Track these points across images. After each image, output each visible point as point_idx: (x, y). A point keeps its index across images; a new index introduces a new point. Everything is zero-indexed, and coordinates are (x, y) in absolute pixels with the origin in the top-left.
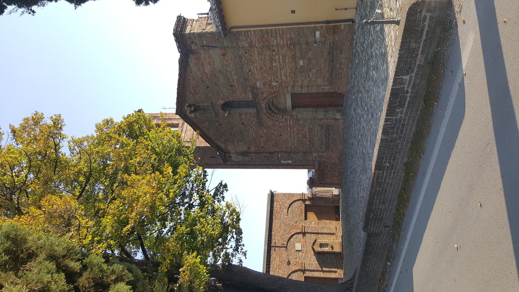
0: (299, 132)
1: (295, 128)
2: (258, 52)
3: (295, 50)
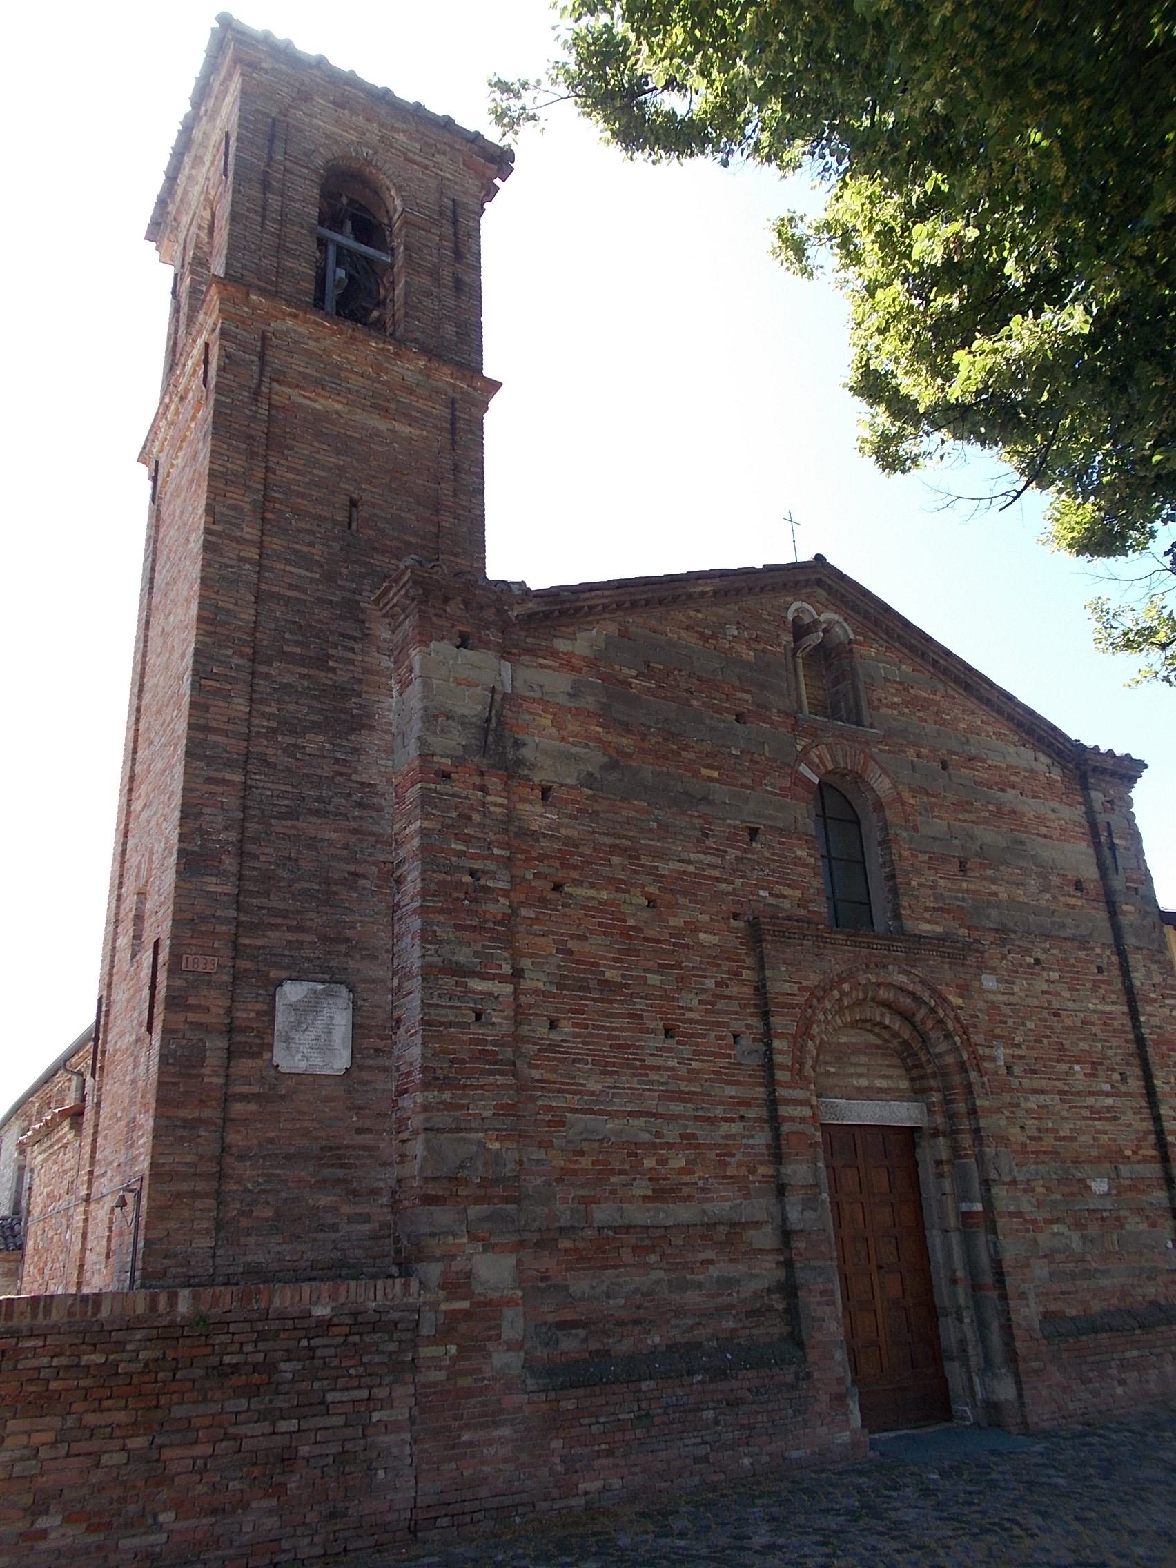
0: (711, 1155)
1: (735, 1128)
3: (1139, 1162)
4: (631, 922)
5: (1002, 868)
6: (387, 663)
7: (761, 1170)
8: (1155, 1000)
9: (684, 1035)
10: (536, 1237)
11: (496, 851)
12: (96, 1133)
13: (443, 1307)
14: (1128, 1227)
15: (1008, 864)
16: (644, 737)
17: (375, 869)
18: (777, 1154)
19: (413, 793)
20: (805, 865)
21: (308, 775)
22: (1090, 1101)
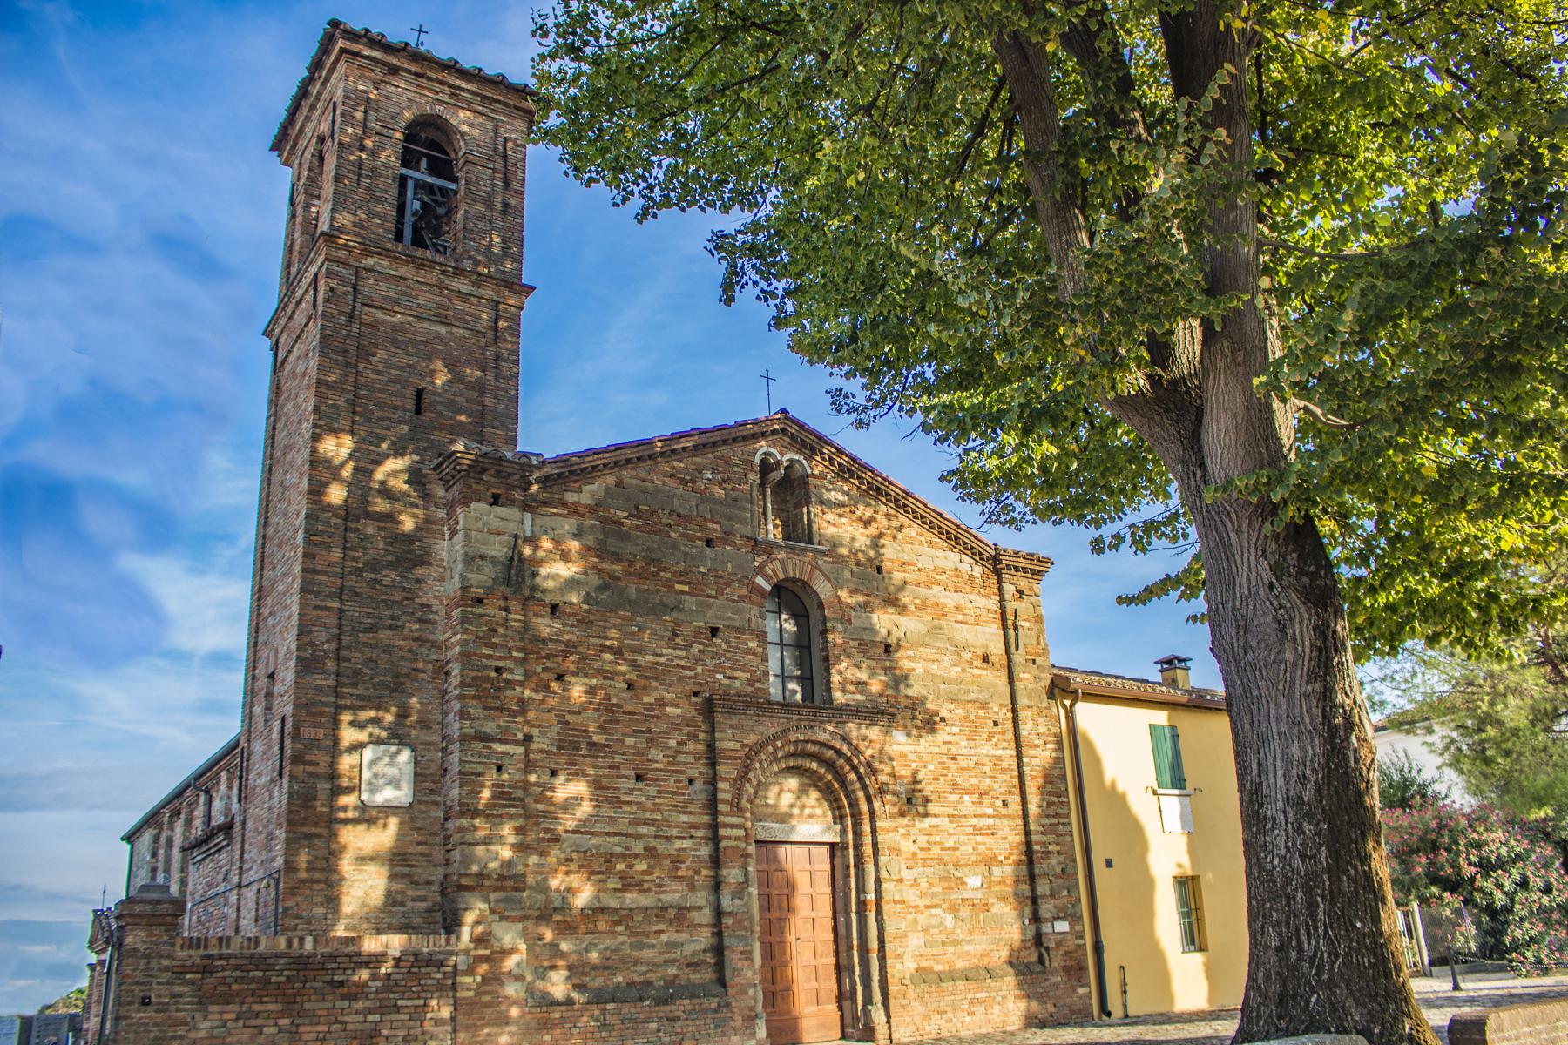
0: (667, 862)
1: (686, 844)
2: (1000, 759)
4: (614, 701)
5: (921, 649)
6: (442, 514)
7: (705, 872)
8: (1038, 746)
9: (651, 779)
10: (537, 913)
11: (515, 654)
12: (243, 842)
13: (473, 953)
14: (994, 910)
15: (926, 646)
16: (631, 563)
17: (430, 666)
18: (716, 862)
19: (456, 613)
20: (754, 654)
21: (384, 601)
22: (974, 821)
